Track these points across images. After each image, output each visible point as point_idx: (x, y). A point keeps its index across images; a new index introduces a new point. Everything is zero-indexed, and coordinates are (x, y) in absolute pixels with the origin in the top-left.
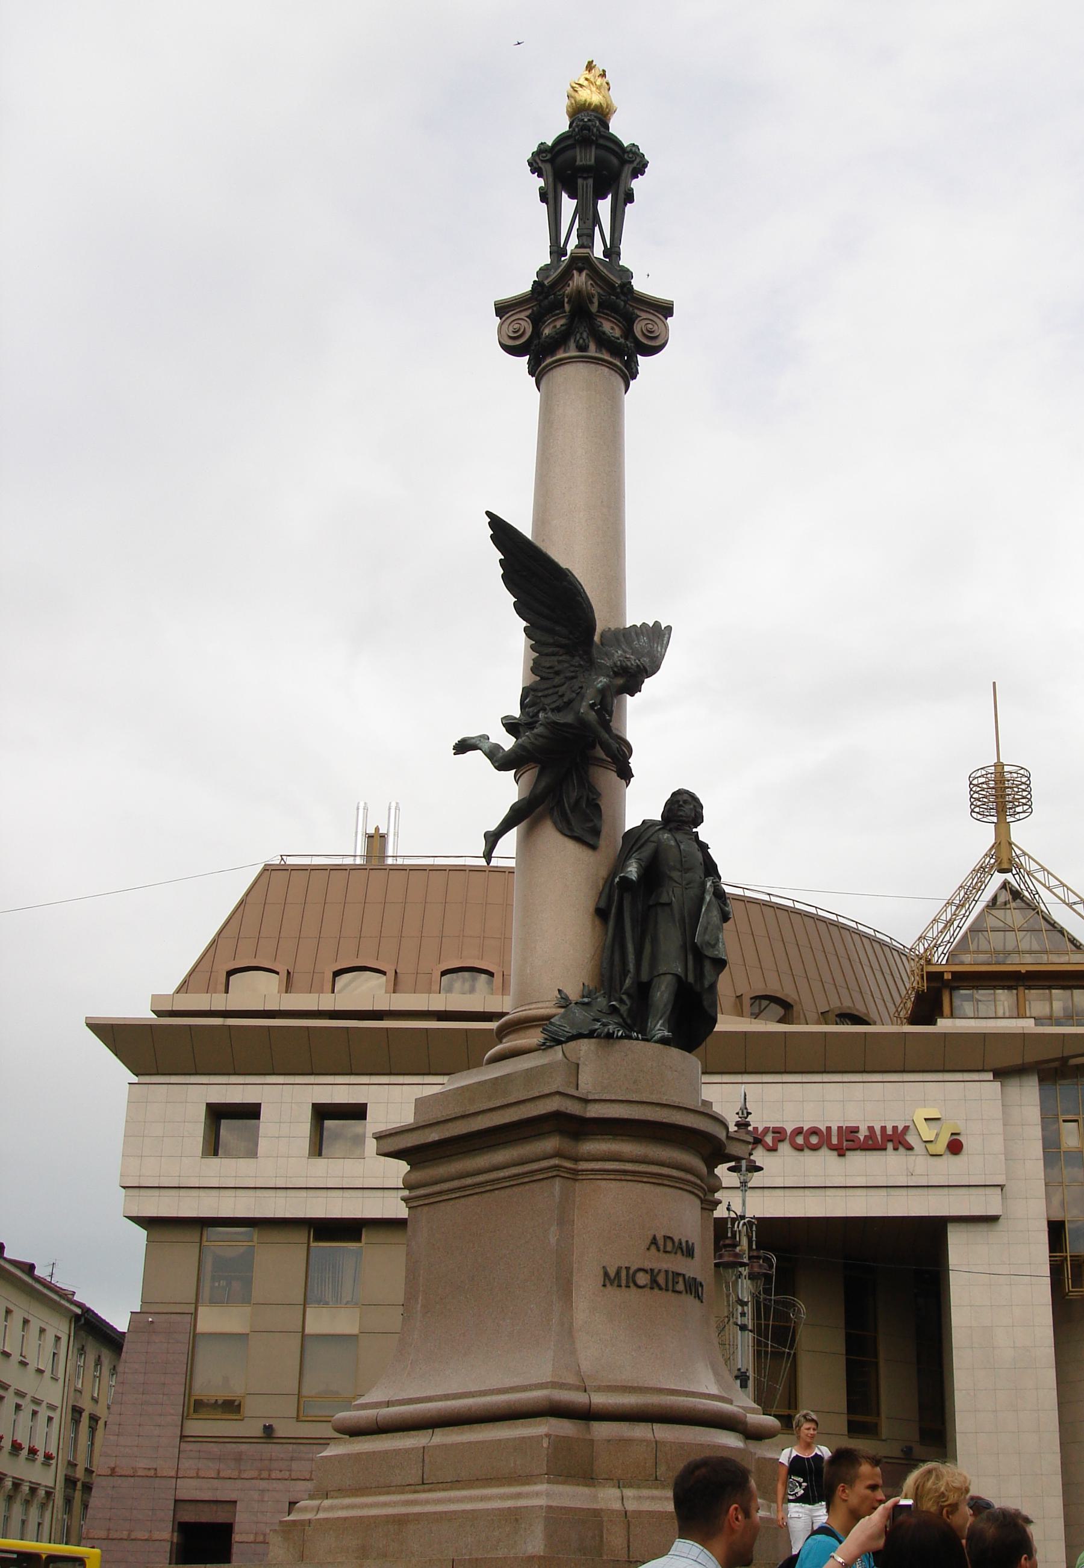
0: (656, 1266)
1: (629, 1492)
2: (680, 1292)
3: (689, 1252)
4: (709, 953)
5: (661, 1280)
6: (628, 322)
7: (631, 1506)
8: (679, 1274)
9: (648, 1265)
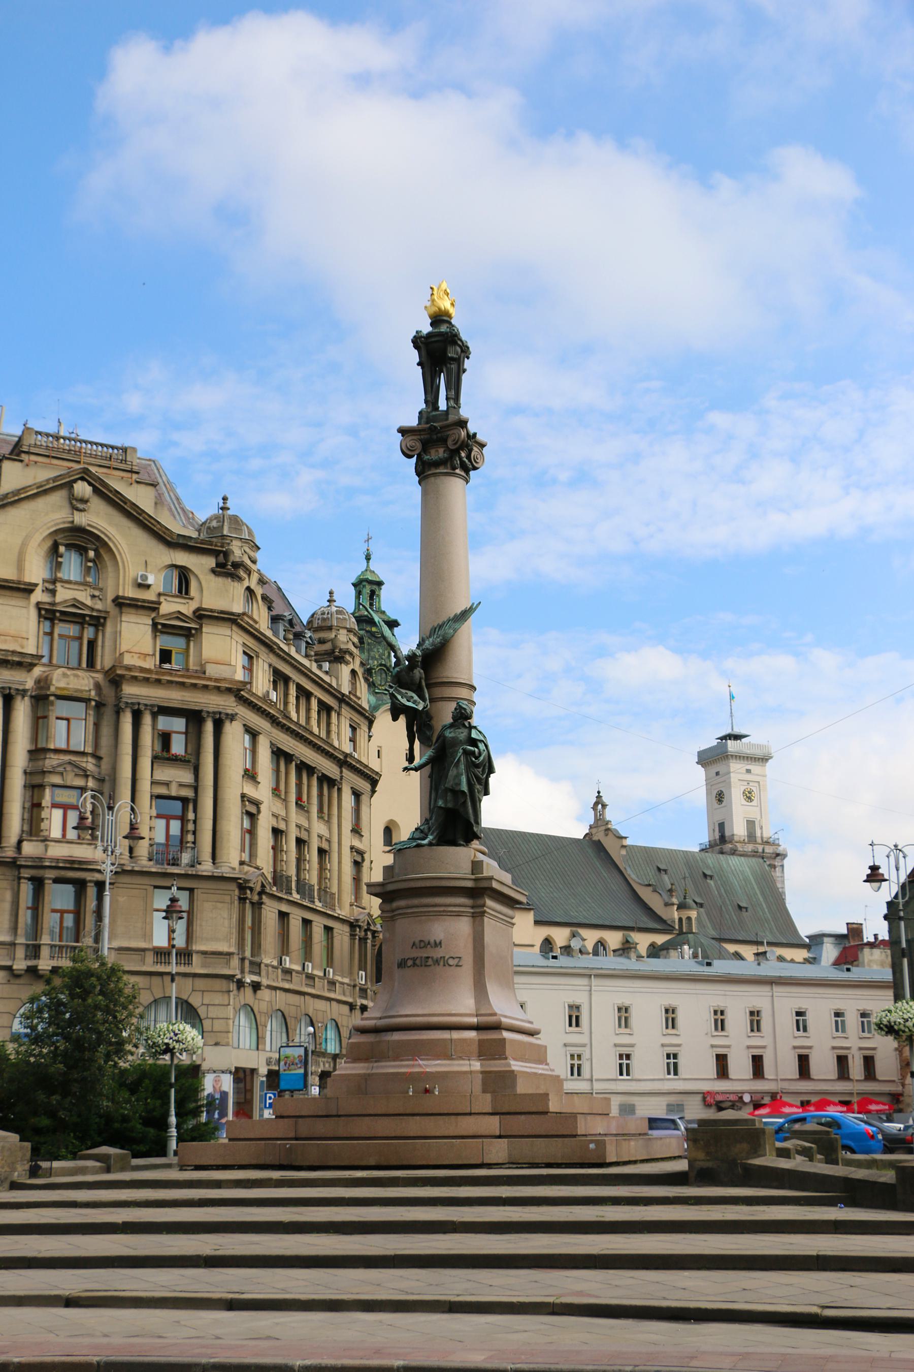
0: (415, 955)
1: (375, 1064)
2: (430, 966)
3: (438, 944)
4: (457, 789)
5: (418, 962)
6: (444, 441)
7: (374, 1071)
8: (428, 958)
9: (412, 956)
